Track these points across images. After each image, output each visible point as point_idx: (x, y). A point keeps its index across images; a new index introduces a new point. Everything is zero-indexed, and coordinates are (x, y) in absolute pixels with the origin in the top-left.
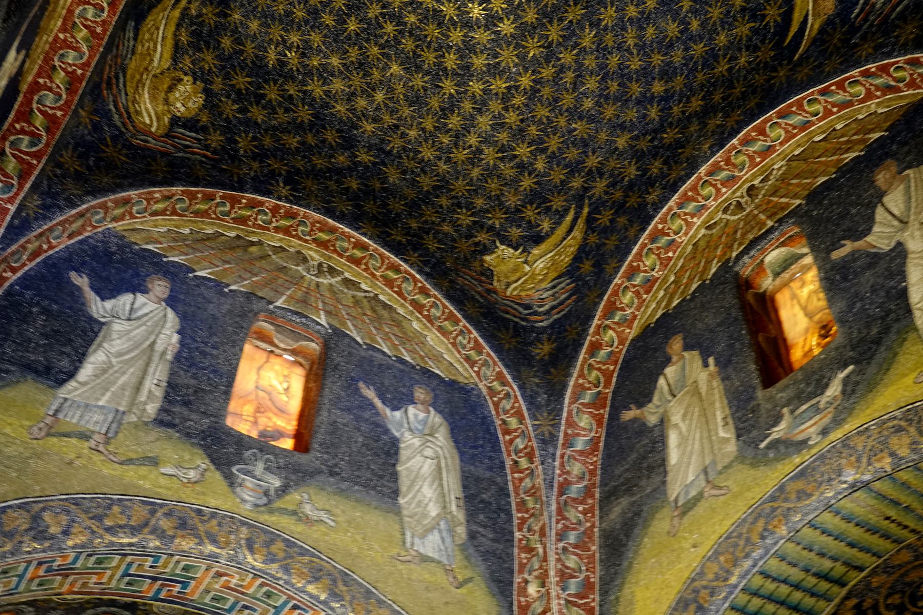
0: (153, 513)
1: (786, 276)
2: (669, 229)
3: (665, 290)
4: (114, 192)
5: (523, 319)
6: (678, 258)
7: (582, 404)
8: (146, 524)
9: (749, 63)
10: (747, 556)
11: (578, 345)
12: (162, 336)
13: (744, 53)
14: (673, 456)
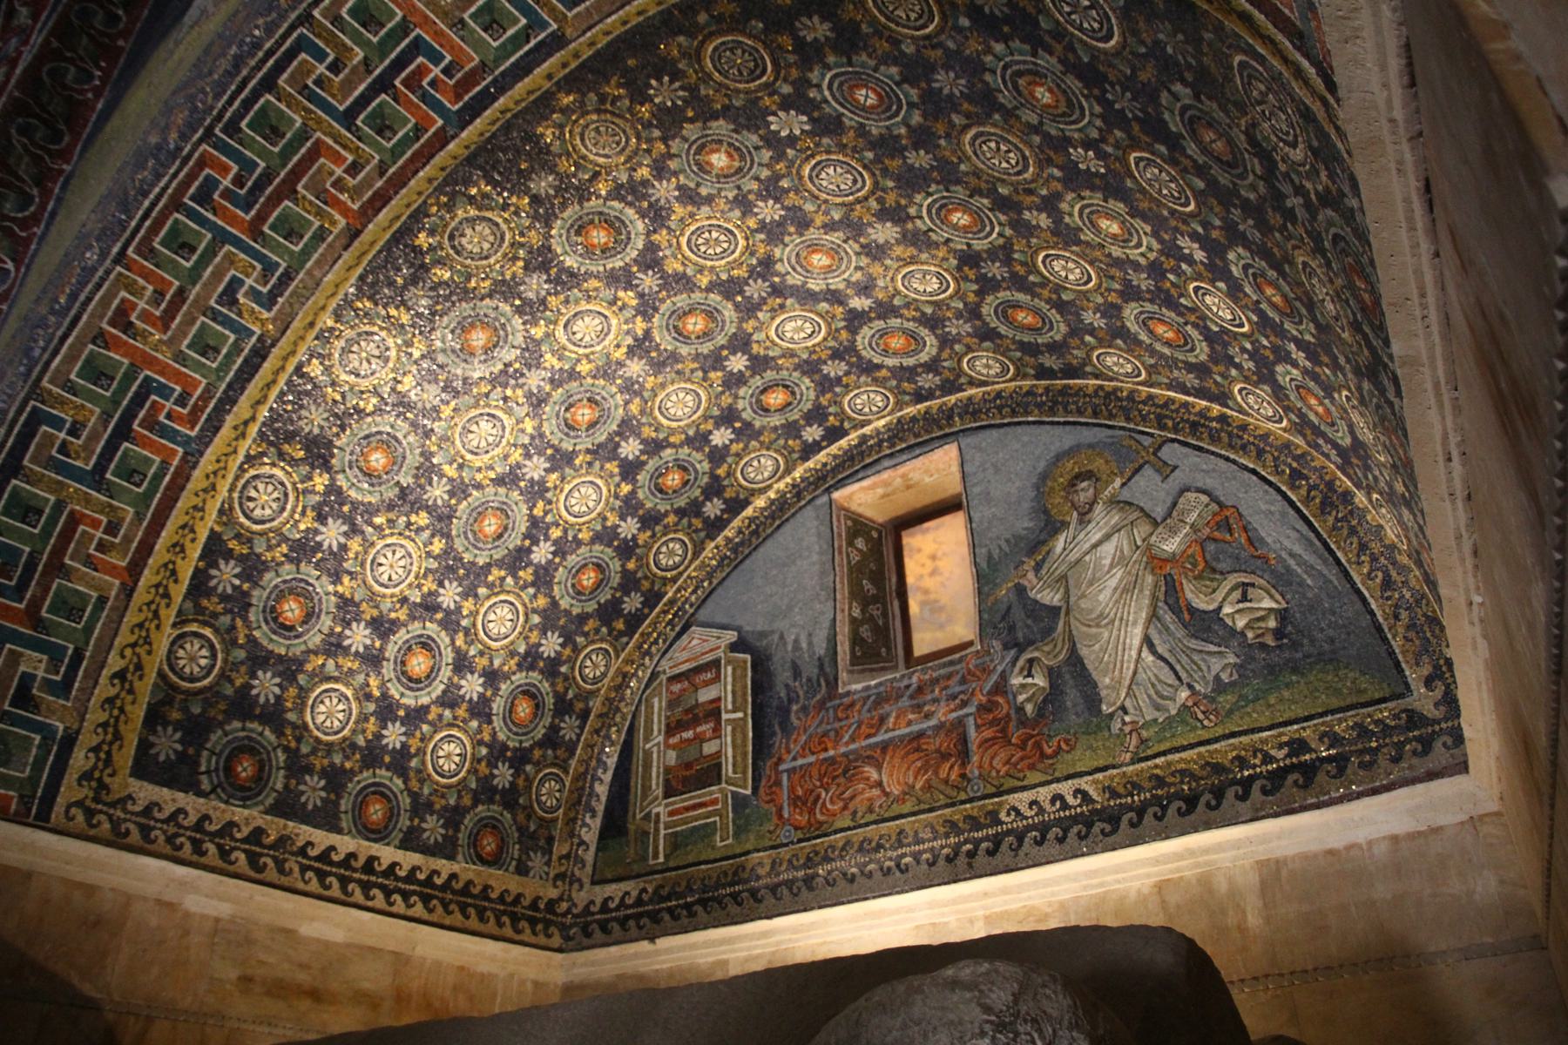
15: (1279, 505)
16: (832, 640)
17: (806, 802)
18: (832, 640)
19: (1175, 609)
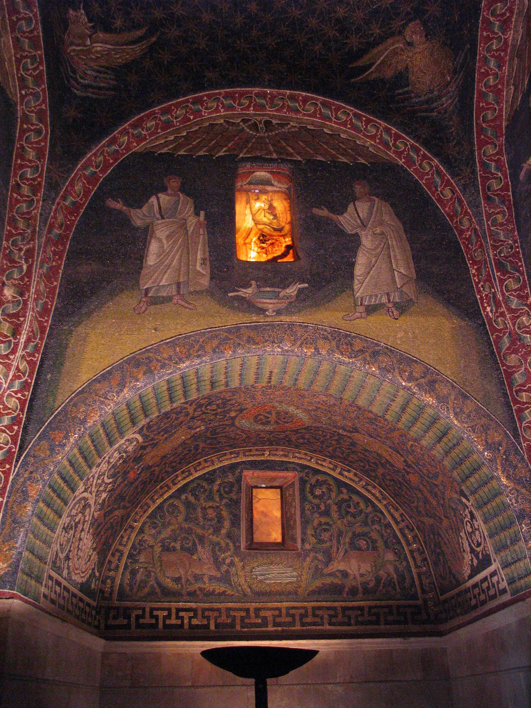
1: (252, 187)
2: (207, 103)
3: (175, 137)
6: (196, 124)
9: (321, 54)
10: (199, 356)
11: (104, 132)
13: (321, 45)
14: (151, 260)
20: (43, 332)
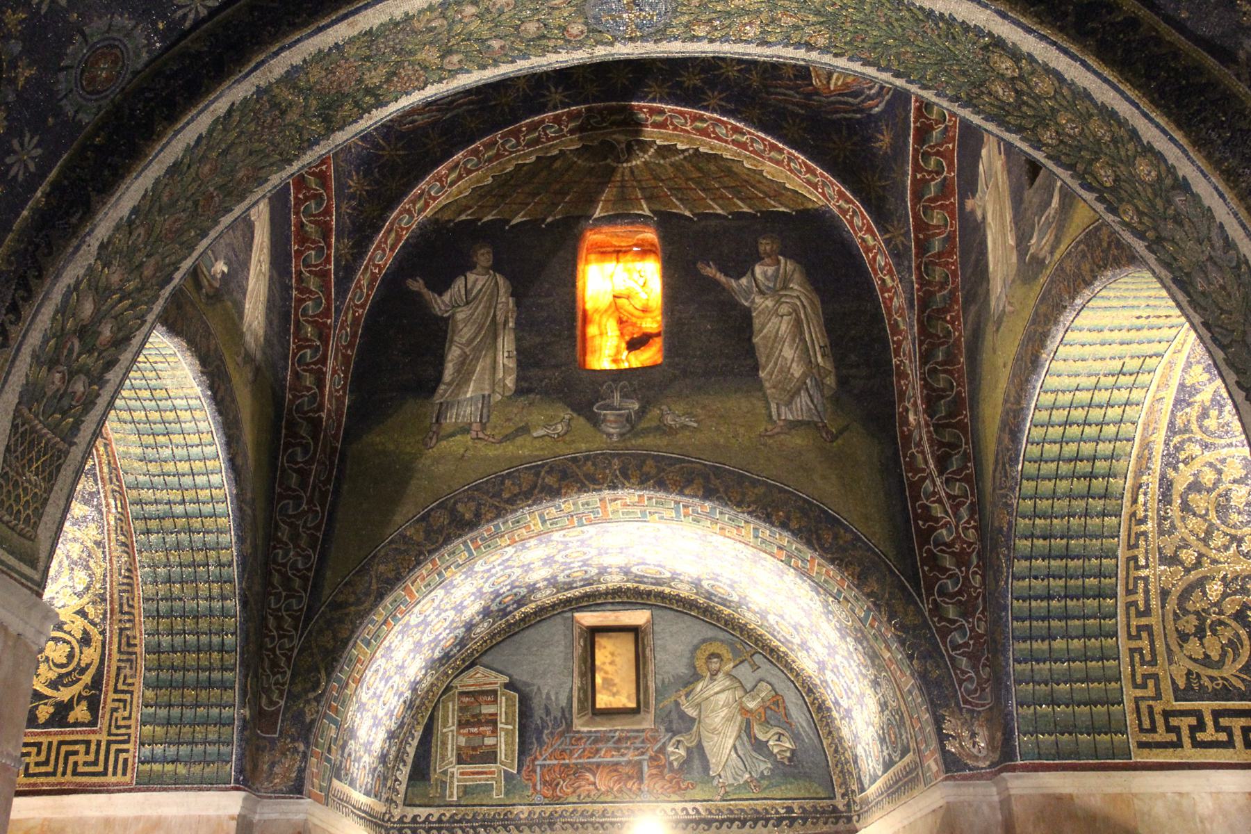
0: (537, 474)
4: (405, 194)
5: (855, 112)
7: (930, 200)
8: (535, 486)
12: (500, 306)
15: (801, 702)
16: (570, 699)
17: (551, 784)
18: (570, 699)
19: (749, 736)
20: (965, 435)
